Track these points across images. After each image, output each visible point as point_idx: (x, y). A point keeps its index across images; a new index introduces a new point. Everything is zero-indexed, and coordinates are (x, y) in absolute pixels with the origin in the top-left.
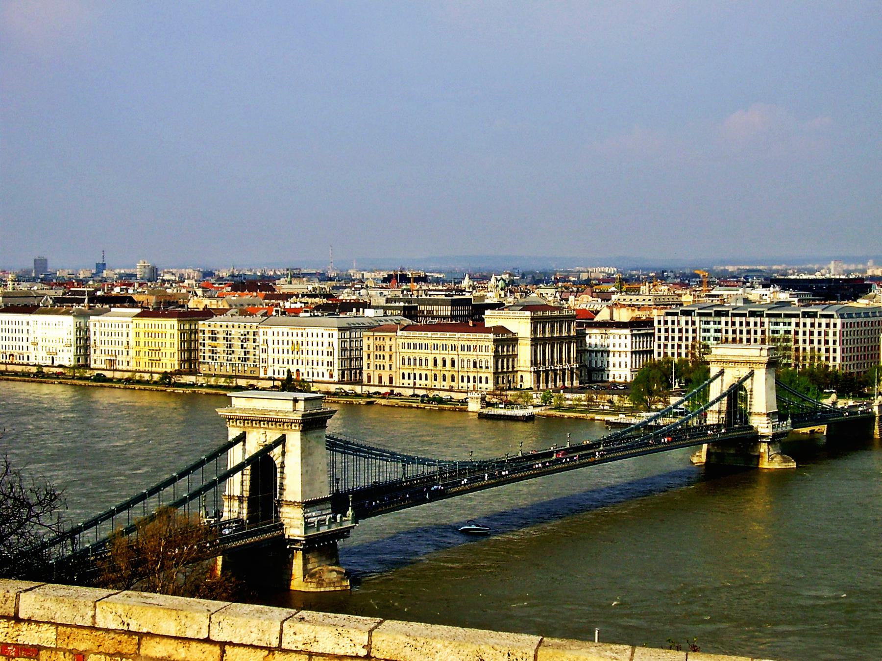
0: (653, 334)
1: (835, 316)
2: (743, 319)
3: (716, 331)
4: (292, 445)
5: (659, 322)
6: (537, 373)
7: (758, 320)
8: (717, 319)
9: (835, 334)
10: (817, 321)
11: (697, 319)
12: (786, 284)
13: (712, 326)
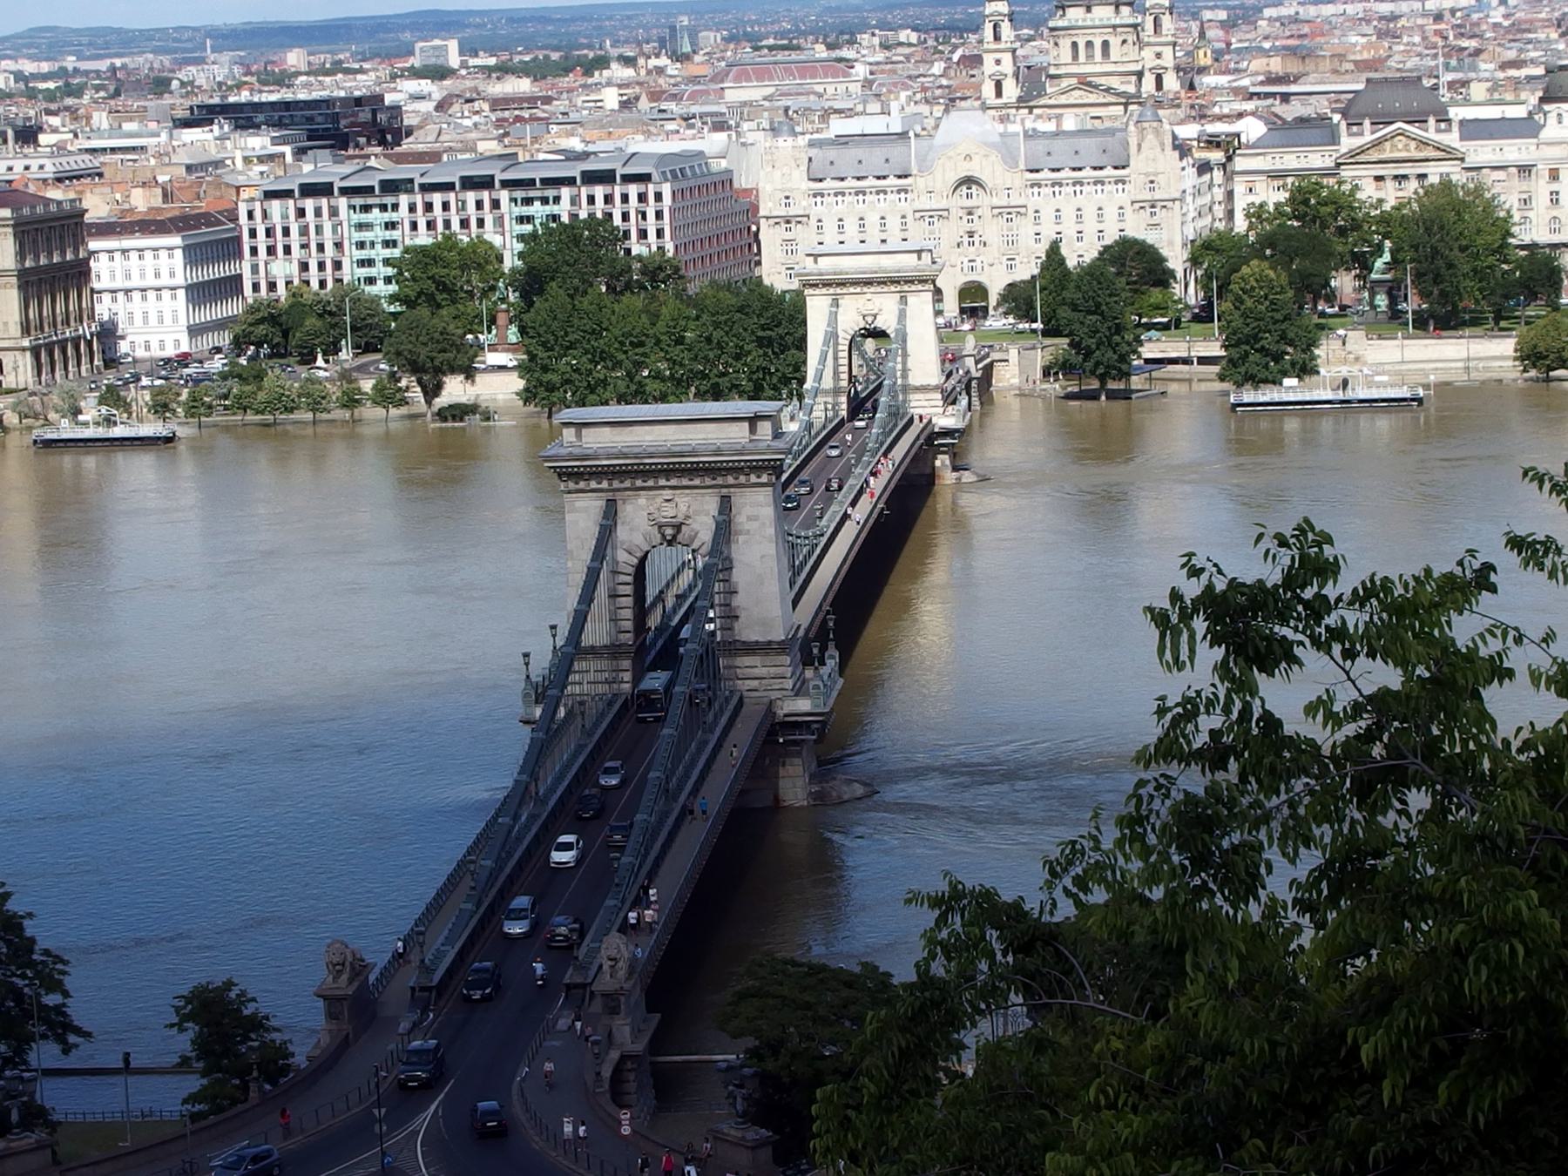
0: (239, 239)
1: (655, 177)
2: (452, 197)
3: (391, 225)
4: (749, 518)
5: (250, 215)
6: (35, 352)
7: (485, 195)
8: (389, 200)
9: (659, 215)
10: (618, 191)
11: (343, 203)
12: (244, 118)
13: (376, 216)
